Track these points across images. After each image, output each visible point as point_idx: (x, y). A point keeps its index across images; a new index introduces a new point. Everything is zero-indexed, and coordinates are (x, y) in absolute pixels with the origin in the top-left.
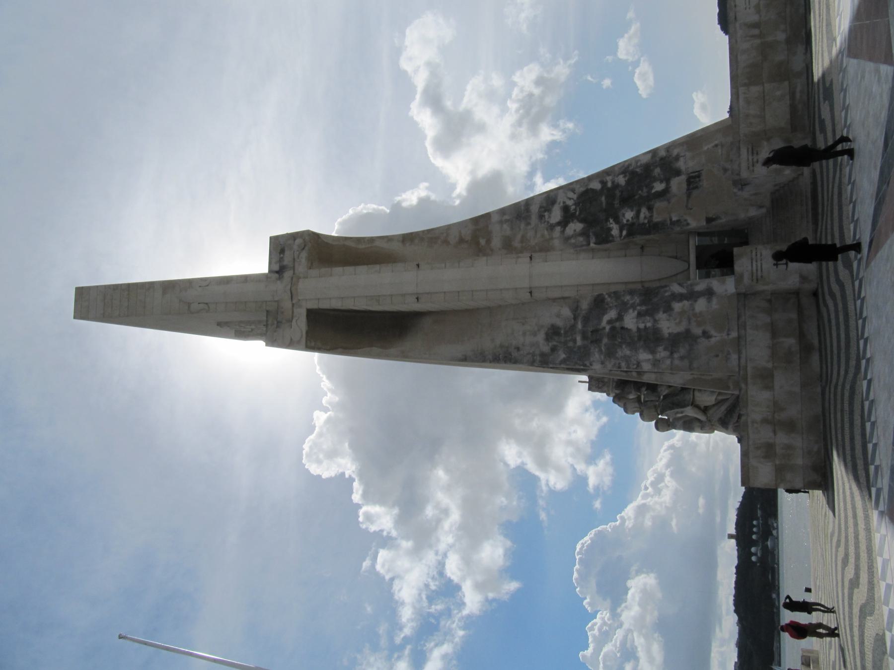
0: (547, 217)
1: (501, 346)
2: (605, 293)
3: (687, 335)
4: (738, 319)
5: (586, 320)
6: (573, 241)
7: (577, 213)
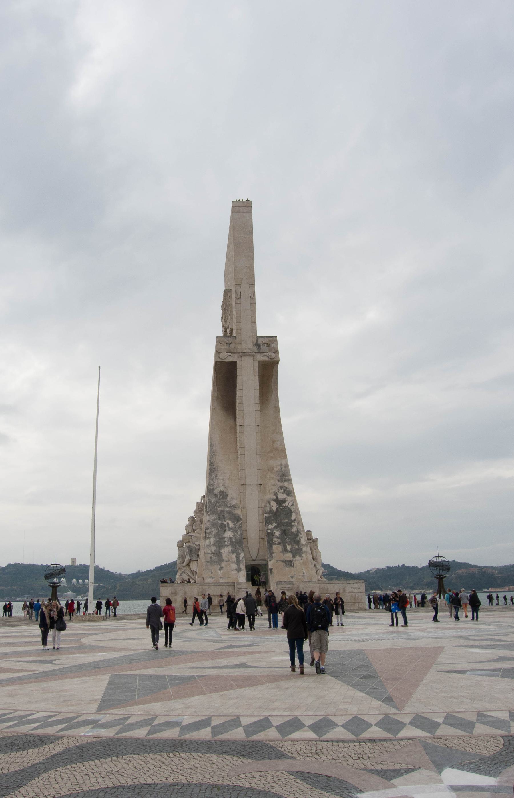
0: (281, 491)
1: (218, 467)
2: (241, 521)
3: (221, 560)
4: (225, 583)
5: (230, 512)
6: (268, 505)
7: (281, 507)
